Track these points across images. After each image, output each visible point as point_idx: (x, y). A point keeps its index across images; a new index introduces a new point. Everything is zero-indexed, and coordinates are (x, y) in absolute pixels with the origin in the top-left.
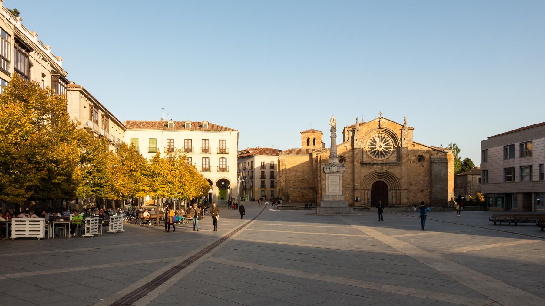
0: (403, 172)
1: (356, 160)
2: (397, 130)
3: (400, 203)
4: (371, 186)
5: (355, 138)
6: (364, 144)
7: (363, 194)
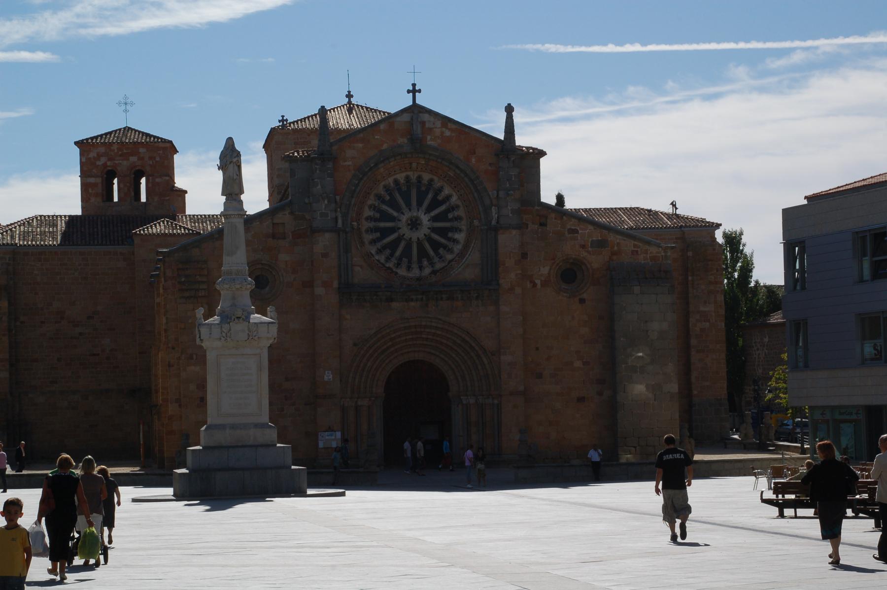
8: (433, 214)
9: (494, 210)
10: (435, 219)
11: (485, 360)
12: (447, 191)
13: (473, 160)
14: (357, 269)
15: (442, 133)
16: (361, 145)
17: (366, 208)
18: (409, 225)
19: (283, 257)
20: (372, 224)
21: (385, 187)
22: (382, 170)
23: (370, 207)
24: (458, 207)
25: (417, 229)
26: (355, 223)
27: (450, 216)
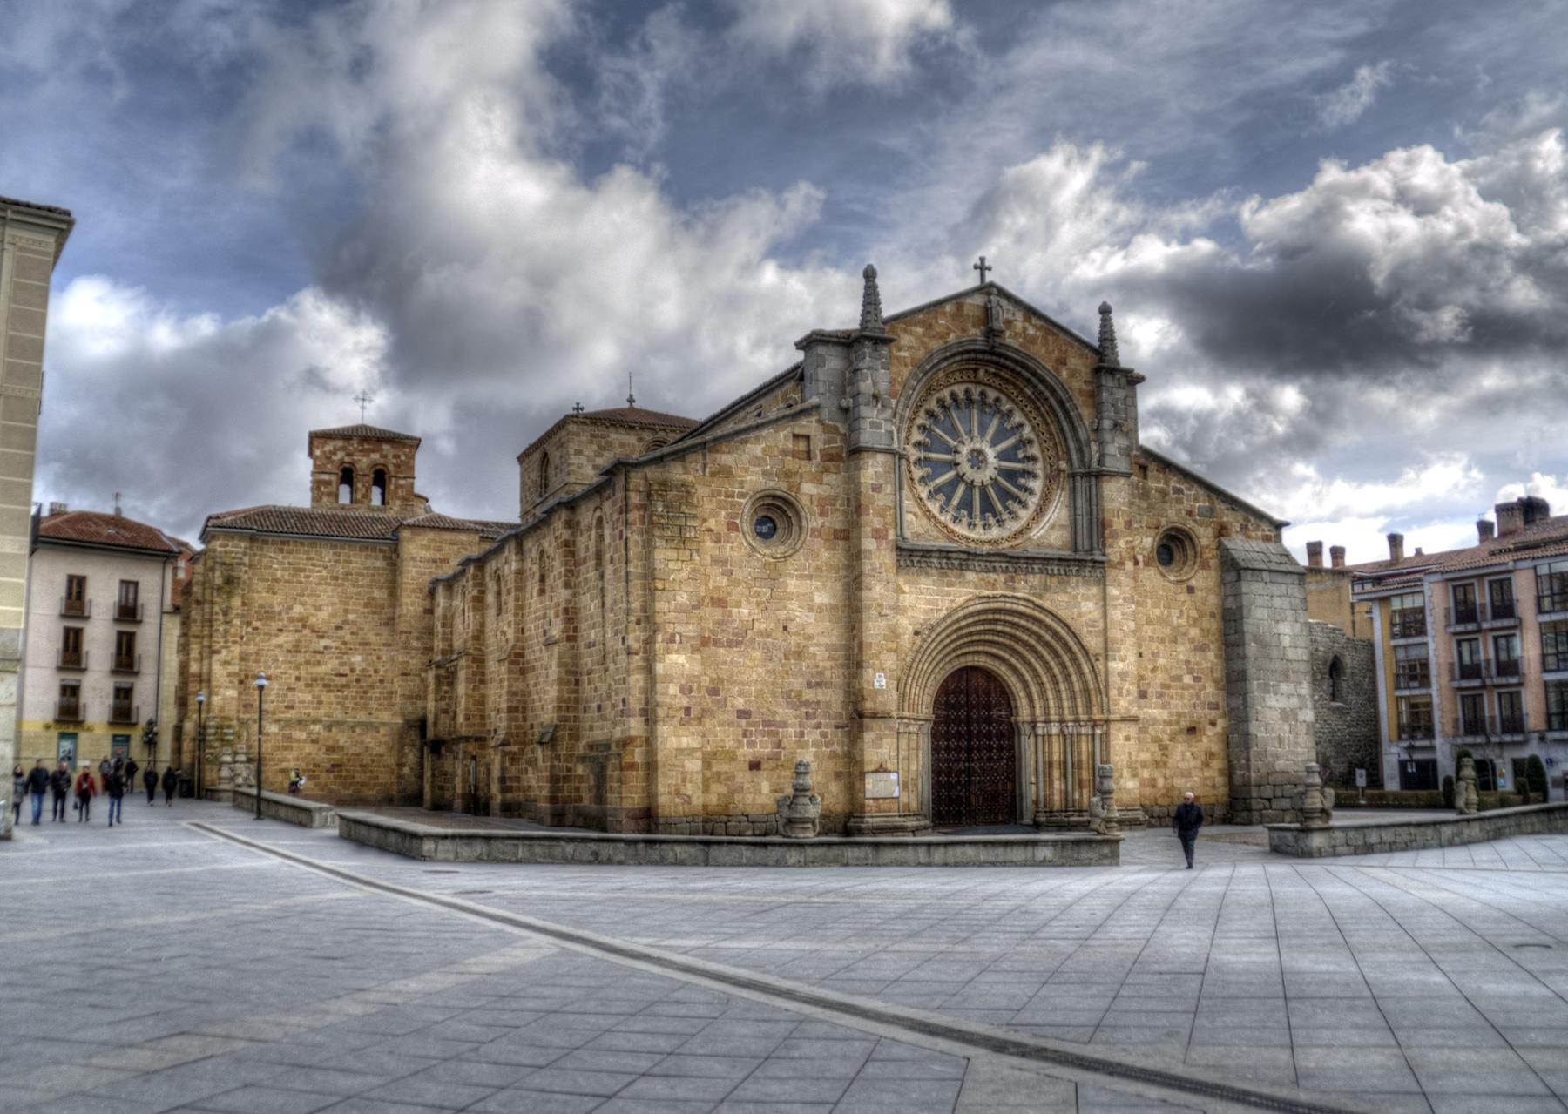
0: (1116, 614)
1: (872, 521)
2: (1072, 374)
5: (866, 386)
6: (904, 435)
8: (1000, 447)
9: (1094, 447)
12: (1018, 418)
13: (1064, 373)
15: (1025, 329)
16: (920, 330)
19: (808, 488)
21: (939, 401)
22: (941, 374)
24: (1030, 442)
27: (1021, 455)
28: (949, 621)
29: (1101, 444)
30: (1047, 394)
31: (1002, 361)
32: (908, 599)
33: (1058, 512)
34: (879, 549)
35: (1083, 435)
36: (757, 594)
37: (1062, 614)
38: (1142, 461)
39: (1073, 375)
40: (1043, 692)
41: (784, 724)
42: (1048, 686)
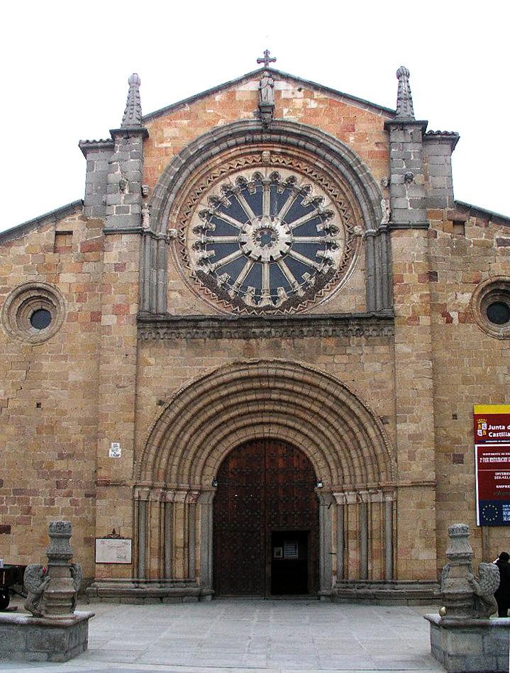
0: (407, 373)
3: (391, 578)
4: (211, 472)
7: (155, 512)
8: (293, 225)
10: (296, 232)
11: (371, 431)
13: (352, 139)
14: (174, 295)
15: (305, 104)
16: (185, 122)
17: (196, 216)
18: (258, 240)
20: (203, 238)
21: (224, 188)
23: (202, 214)
24: (330, 214)
25: (270, 246)
26: (174, 231)
27: (320, 228)
28: (200, 390)
29: (391, 199)
30: (336, 162)
31: (283, 138)
32: (148, 372)
33: (355, 278)
34: (119, 323)
35: (373, 195)
36: (13, 376)
37: (338, 376)
38: (459, 216)
39: (363, 141)
40: (338, 463)
41: (35, 492)
42: (341, 454)
